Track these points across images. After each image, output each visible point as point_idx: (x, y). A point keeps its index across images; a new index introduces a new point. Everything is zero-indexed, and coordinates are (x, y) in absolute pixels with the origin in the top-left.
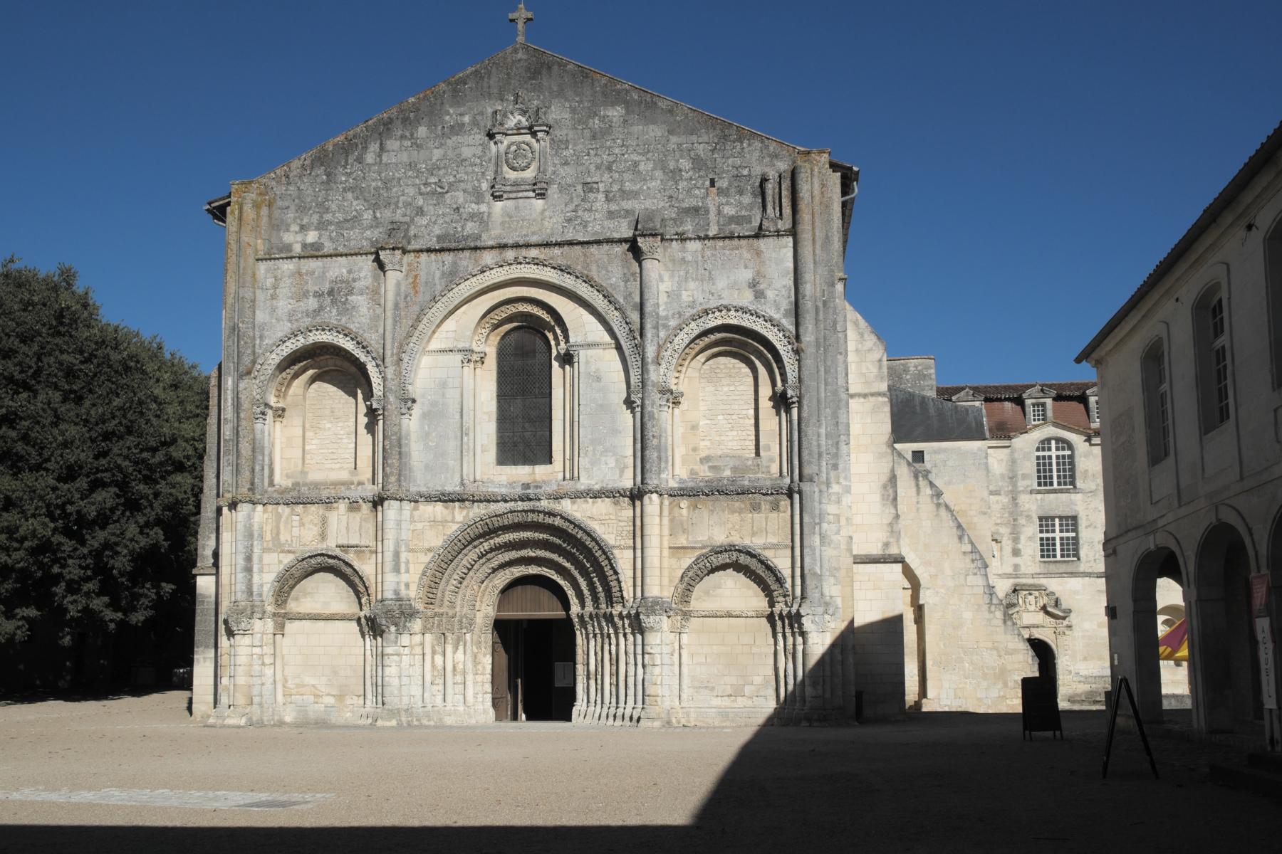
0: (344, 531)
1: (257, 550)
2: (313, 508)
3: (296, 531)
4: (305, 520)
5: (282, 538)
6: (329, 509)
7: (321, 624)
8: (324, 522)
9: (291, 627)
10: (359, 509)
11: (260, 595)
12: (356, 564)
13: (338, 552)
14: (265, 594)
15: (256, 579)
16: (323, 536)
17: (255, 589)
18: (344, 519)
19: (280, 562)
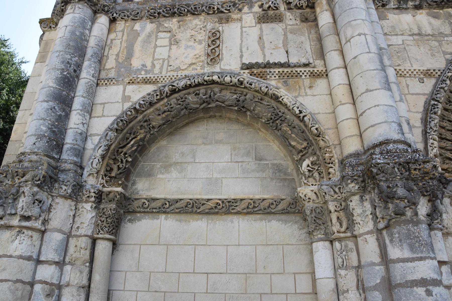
0: (255, 46)
1: (86, 75)
2: (195, 22)
3: (162, 53)
4: (179, 36)
5: (136, 63)
6: (228, 20)
7: (199, 225)
8: (215, 39)
9: (139, 230)
10: (279, 19)
11: (80, 153)
12: (287, 96)
13: (246, 76)
14: (88, 153)
15: (75, 120)
16: (213, 56)
17: (69, 139)
18: (254, 32)
19: (126, 98)
